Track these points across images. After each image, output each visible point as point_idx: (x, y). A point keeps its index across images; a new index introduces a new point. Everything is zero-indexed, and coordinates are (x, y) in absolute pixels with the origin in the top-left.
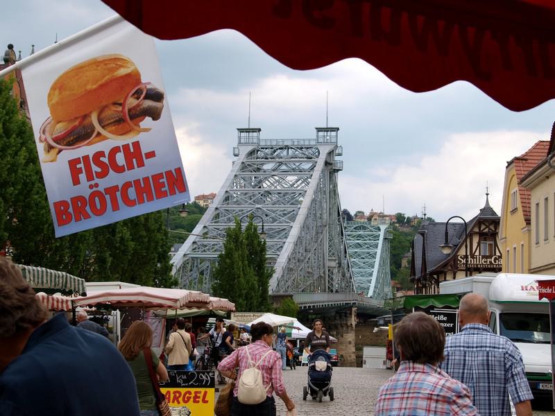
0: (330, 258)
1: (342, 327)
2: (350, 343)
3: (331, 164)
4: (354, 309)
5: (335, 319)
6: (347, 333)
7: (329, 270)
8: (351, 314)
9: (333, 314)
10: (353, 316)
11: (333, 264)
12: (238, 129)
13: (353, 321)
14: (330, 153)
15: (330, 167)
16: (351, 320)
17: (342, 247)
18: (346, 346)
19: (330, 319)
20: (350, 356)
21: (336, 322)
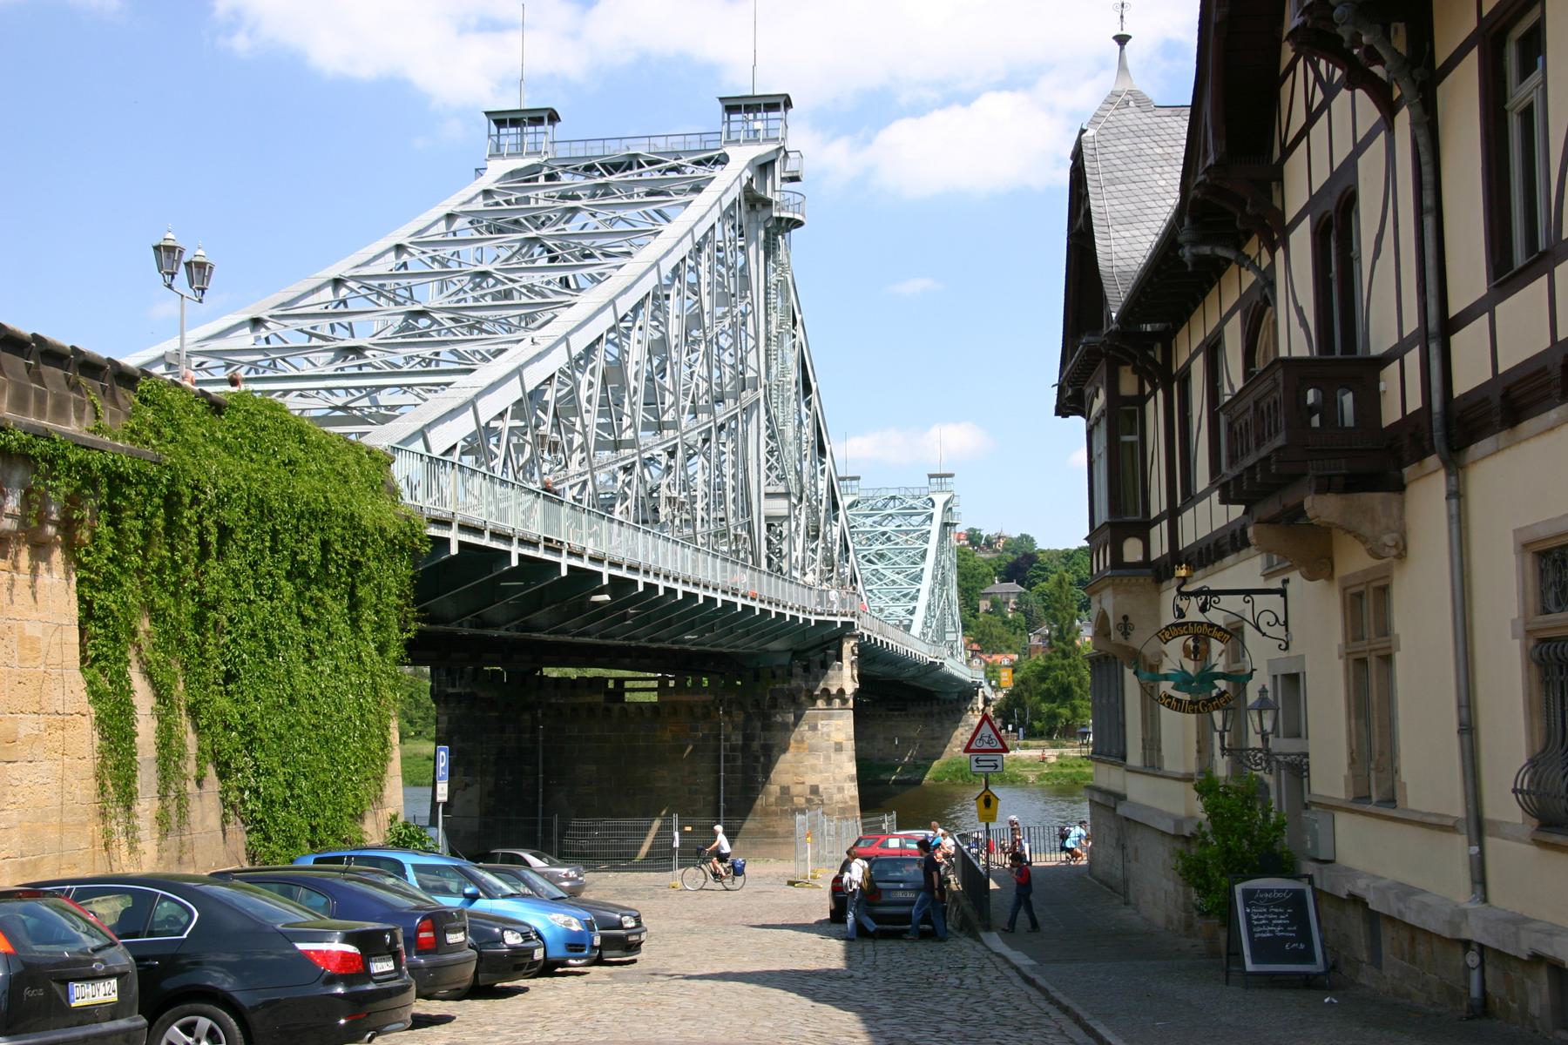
0: (771, 490)
1: (813, 700)
2: (839, 748)
3: (768, 203)
4: (848, 646)
5: (790, 674)
6: (830, 717)
7: (769, 526)
8: (839, 658)
9: (785, 659)
10: (846, 663)
11: (780, 507)
12: (487, 113)
13: (845, 678)
14: (764, 167)
15: (764, 215)
16: (841, 678)
17: (823, 485)
18: (828, 758)
19: (774, 676)
20: (841, 790)
21: (794, 683)
